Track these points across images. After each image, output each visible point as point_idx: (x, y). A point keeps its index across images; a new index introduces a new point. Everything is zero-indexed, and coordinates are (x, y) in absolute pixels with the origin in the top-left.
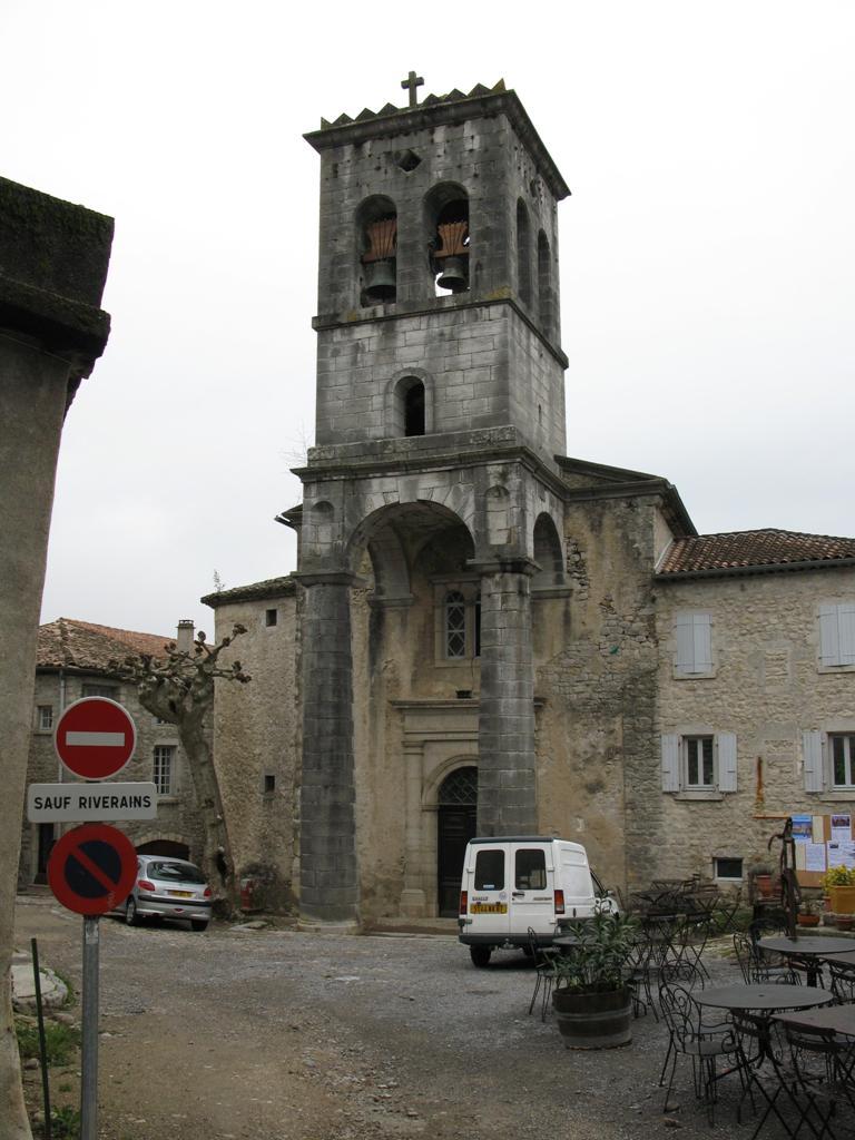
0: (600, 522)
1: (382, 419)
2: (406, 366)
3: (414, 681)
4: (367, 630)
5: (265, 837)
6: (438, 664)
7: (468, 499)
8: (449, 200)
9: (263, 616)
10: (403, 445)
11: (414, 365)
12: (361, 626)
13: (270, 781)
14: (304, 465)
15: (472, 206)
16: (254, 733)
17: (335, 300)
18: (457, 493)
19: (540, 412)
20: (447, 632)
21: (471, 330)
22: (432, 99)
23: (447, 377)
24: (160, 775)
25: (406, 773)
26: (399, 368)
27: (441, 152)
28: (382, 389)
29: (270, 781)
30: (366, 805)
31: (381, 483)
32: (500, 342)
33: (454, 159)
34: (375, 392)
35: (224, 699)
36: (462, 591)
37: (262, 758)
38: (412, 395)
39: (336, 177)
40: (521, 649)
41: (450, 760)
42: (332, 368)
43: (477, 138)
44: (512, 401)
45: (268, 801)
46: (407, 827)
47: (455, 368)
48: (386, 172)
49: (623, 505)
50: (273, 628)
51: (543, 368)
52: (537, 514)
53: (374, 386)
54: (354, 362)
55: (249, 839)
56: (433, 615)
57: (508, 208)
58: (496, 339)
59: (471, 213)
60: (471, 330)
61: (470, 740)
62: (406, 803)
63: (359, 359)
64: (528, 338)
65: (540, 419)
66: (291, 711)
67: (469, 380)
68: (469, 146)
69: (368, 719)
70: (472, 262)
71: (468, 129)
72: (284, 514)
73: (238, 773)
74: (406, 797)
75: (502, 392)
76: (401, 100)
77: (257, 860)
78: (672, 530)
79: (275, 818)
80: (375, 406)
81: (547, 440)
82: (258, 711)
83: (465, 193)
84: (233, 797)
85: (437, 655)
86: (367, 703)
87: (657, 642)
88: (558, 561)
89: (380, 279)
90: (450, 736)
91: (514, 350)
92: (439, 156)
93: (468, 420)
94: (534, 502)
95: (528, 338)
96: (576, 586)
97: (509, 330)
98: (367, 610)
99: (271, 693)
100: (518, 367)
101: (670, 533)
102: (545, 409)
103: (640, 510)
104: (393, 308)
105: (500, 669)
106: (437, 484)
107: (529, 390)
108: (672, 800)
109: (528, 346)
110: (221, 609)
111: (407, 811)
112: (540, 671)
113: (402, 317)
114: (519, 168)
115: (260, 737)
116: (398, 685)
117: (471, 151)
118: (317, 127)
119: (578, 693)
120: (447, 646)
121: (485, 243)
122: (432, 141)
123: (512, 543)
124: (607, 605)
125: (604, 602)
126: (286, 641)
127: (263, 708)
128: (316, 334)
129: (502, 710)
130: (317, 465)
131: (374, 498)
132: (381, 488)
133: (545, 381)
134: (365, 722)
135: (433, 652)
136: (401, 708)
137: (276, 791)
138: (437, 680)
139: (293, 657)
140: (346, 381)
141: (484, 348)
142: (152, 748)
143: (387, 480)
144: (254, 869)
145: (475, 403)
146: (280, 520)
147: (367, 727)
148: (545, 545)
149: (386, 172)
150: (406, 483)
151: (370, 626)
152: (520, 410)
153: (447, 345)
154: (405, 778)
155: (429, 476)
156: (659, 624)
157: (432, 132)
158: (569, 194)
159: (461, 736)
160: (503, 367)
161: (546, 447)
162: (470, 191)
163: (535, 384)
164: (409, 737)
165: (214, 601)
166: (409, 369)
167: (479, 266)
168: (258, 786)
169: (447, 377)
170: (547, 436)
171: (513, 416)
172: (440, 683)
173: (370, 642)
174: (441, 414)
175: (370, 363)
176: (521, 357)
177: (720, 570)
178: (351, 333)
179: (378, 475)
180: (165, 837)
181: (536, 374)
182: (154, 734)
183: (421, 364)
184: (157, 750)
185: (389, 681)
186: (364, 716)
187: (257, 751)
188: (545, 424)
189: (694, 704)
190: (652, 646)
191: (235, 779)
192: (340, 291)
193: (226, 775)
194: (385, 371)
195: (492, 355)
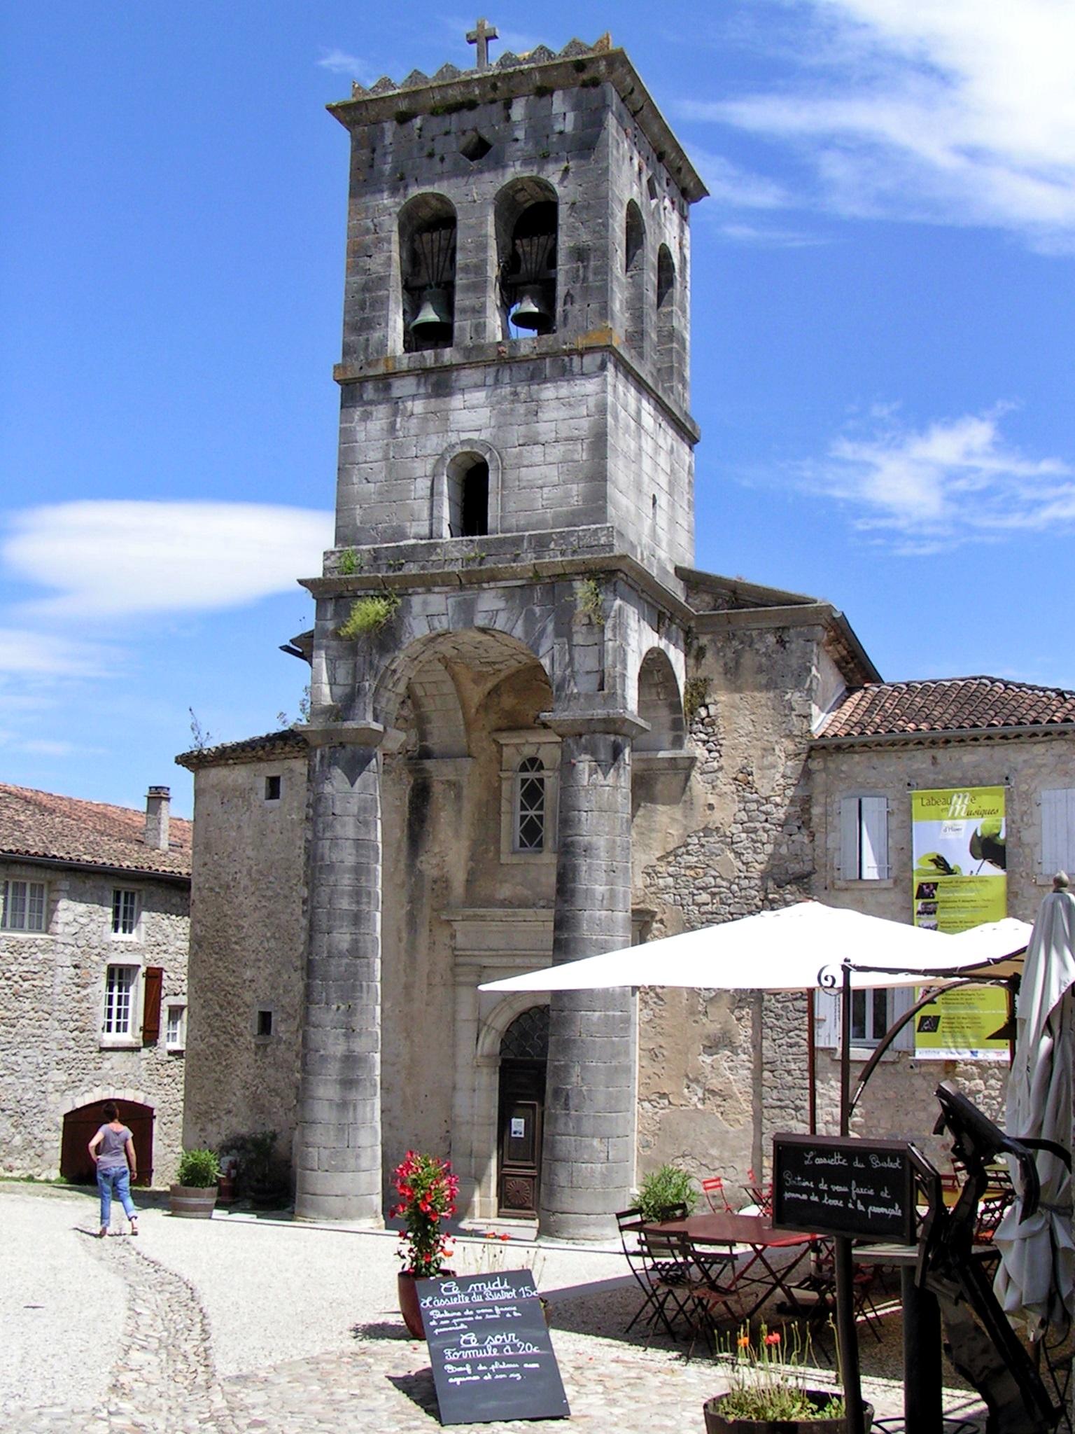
0: (737, 663)
1: (429, 513)
2: (464, 436)
3: (469, 882)
4: (406, 809)
7: (544, 629)
8: (532, 202)
9: (262, 784)
10: (455, 548)
11: (474, 436)
13: (265, 1021)
14: (317, 573)
15: (563, 211)
16: (244, 950)
17: (367, 340)
18: (530, 619)
19: (654, 504)
20: (519, 813)
21: (557, 388)
22: (507, 59)
23: (521, 453)
24: (115, 1007)
25: (454, 1012)
26: (453, 438)
27: (520, 134)
28: (429, 469)
29: (265, 1018)
31: (425, 603)
32: (596, 406)
33: (537, 144)
34: (419, 472)
35: (203, 901)
36: (541, 756)
37: (254, 986)
38: (473, 484)
39: (372, 166)
40: (614, 842)
42: (361, 436)
43: (571, 116)
44: (610, 488)
46: (454, 1088)
47: (532, 441)
48: (442, 160)
49: (771, 639)
50: (275, 803)
51: (661, 442)
52: (645, 650)
53: (418, 464)
54: (392, 428)
55: (234, 1099)
56: (500, 787)
57: (613, 215)
58: (592, 401)
59: (560, 222)
60: (557, 388)
62: (454, 1055)
63: (398, 426)
64: (639, 401)
65: (654, 514)
66: (297, 920)
67: (549, 459)
68: (558, 127)
69: (404, 935)
70: (561, 291)
71: (558, 102)
72: (291, 641)
73: (221, 1007)
74: (454, 1046)
75: (598, 476)
76: (467, 64)
78: (845, 675)
79: (271, 1071)
80: (420, 493)
81: (664, 545)
83: (553, 192)
84: (214, 1040)
85: (504, 846)
87: (812, 835)
88: (677, 716)
89: (429, 315)
91: (616, 418)
92: (517, 140)
93: (549, 514)
94: (640, 632)
95: (639, 401)
96: (700, 752)
97: (610, 388)
99: (269, 893)
100: (621, 441)
101: (841, 678)
102: (663, 500)
103: (794, 646)
104: (449, 355)
105: (584, 868)
106: (501, 604)
107: (638, 475)
108: (828, 1060)
109: (639, 412)
110: (202, 772)
111: (455, 1067)
112: (651, 872)
113: (459, 367)
114: (631, 159)
116: (446, 888)
117: (561, 133)
118: (347, 97)
119: (699, 905)
120: (518, 833)
121: (580, 264)
122: (508, 118)
123: (606, 691)
124: (744, 780)
125: (740, 776)
127: (256, 915)
128: (338, 388)
129: (585, 927)
130: (336, 576)
131: (414, 623)
132: (424, 610)
133: (663, 460)
134: (400, 940)
135: (498, 841)
137: (273, 1033)
138: (501, 882)
139: (302, 843)
140: (380, 456)
141: (573, 413)
142: (105, 969)
143: (432, 598)
144: (239, 1144)
145: (559, 492)
146: (287, 649)
147: (403, 944)
148: (658, 694)
149: (442, 160)
150: (459, 604)
151: (411, 802)
152: (623, 502)
153: (521, 409)
154: (454, 1019)
155: (493, 593)
156: (816, 810)
157: (508, 105)
158: (708, 195)
160: (599, 442)
161: (662, 554)
162: (559, 190)
163: (647, 465)
165: (194, 761)
166: (469, 441)
167: (569, 297)
168: (249, 1026)
169: (520, 454)
170: (663, 536)
171: (611, 510)
174: (512, 506)
175: (412, 432)
176: (628, 426)
177: (902, 736)
178: (388, 387)
179: (420, 590)
180: (119, 1095)
181: (650, 451)
182: (109, 947)
183: (484, 435)
184: (111, 970)
185: (435, 882)
186: (399, 931)
187: (248, 974)
188: (662, 520)
190: (806, 840)
191: (217, 1015)
192: (373, 328)
193: (203, 1007)
194: (434, 444)
195: (585, 424)
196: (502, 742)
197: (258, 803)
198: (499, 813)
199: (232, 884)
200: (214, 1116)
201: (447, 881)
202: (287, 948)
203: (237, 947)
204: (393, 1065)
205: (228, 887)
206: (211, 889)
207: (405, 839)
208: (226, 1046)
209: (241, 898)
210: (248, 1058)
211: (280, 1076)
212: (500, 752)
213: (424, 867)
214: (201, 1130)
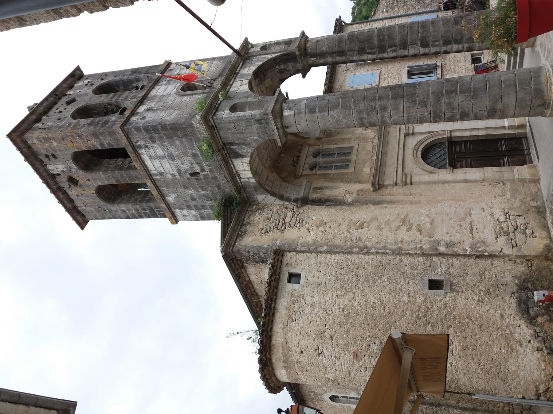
5: (488, 292)
6: (352, 170)
12: (317, 211)
13: (435, 285)
16: (389, 302)
41: (415, 156)
45: (453, 288)
55: (492, 311)
56: (320, 175)
61: (404, 155)
73: (428, 323)
77: (513, 301)
82: (369, 295)
86: (372, 206)
90: (400, 162)
98: (307, 207)
115: (393, 294)
116: (362, 190)
126: (316, 264)
134: (386, 207)
136: (378, 186)
137: (442, 278)
138: (362, 171)
147: (389, 206)
159: (401, 157)
164: (399, 182)
172: (364, 170)
173: (329, 205)
186: (381, 208)
187: (405, 299)
189: (392, 78)
196: (300, 174)
197: (300, 289)
199: (346, 312)
200: (508, 331)
202: (388, 267)
203: (387, 308)
204: (456, 208)
205: (348, 315)
206: (348, 332)
208: (455, 318)
209: (356, 304)
210: (461, 300)
211: (470, 272)
212: (304, 175)
213: (350, 200)
214: (521, 345)
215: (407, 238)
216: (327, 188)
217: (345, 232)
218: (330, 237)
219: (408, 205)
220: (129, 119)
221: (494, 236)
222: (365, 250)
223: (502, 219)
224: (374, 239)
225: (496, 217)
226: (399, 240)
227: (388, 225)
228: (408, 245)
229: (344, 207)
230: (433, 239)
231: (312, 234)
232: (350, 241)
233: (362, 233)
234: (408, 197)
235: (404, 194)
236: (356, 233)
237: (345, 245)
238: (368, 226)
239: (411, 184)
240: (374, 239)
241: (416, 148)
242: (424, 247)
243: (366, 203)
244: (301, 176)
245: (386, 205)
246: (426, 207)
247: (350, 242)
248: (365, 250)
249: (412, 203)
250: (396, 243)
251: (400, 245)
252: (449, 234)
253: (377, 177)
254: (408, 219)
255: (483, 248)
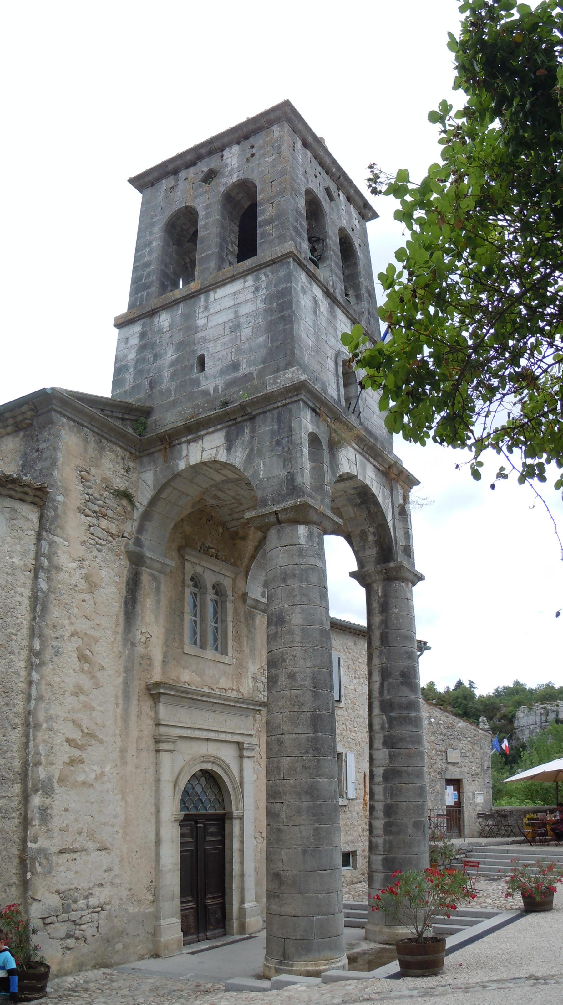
3: (164, 663)
4: (124, 587)
12: (117, 579)
30: (115, 817)
41: (204, 759)
56: (183, 593)
61: (208, 740)
69: (121, 701)
86: (120, 680)
90: (197, 734)
134: (117, 705)
136: (155, 693)
138: (184, 668)
147: (119, 711)
151: (128, 583)
164: (162, 730)
172: (187, 671)
173: (126, 603)
186: (117, 697)
196: (186, 557)
198: (183, 613)
201: (150, 659)
207: (122, 614)
212: (183, 564)
215: (58, 739)
216: (158, 602)
217: (72, 628)
218: (65, 598)
219: (119, 744)
220: (303, 269)
221: (62, 888)
222: (35, 659)
223: (93, 901)
224: (58, 680)
225: (96, 891)
226: (54, 724)
227: (84, 706)
228: (44, 741)
229: (121, 629)
230: (55, 785)
231: (74, 565)
232: (56, 635)
233: (70, 658)
234: (135, 745)
235: (139, 738)
236: (71, 647)
237: (47, 625)
238: (83, 671)
239: (158, 751)
240: (58, 680)
241: (219, 762)
242: (41, 769)
243: (128, 670)
244: (182, 558)
245: (121, 706)
246: (115, 775)
247: (53, 635)
248: (35, 659)
249: (123, 750)
250: (49, 718)
251: (45, 726)
252: (64, 813)
253: (172, 693)
254: (93, 742)
255: (39, 869)
